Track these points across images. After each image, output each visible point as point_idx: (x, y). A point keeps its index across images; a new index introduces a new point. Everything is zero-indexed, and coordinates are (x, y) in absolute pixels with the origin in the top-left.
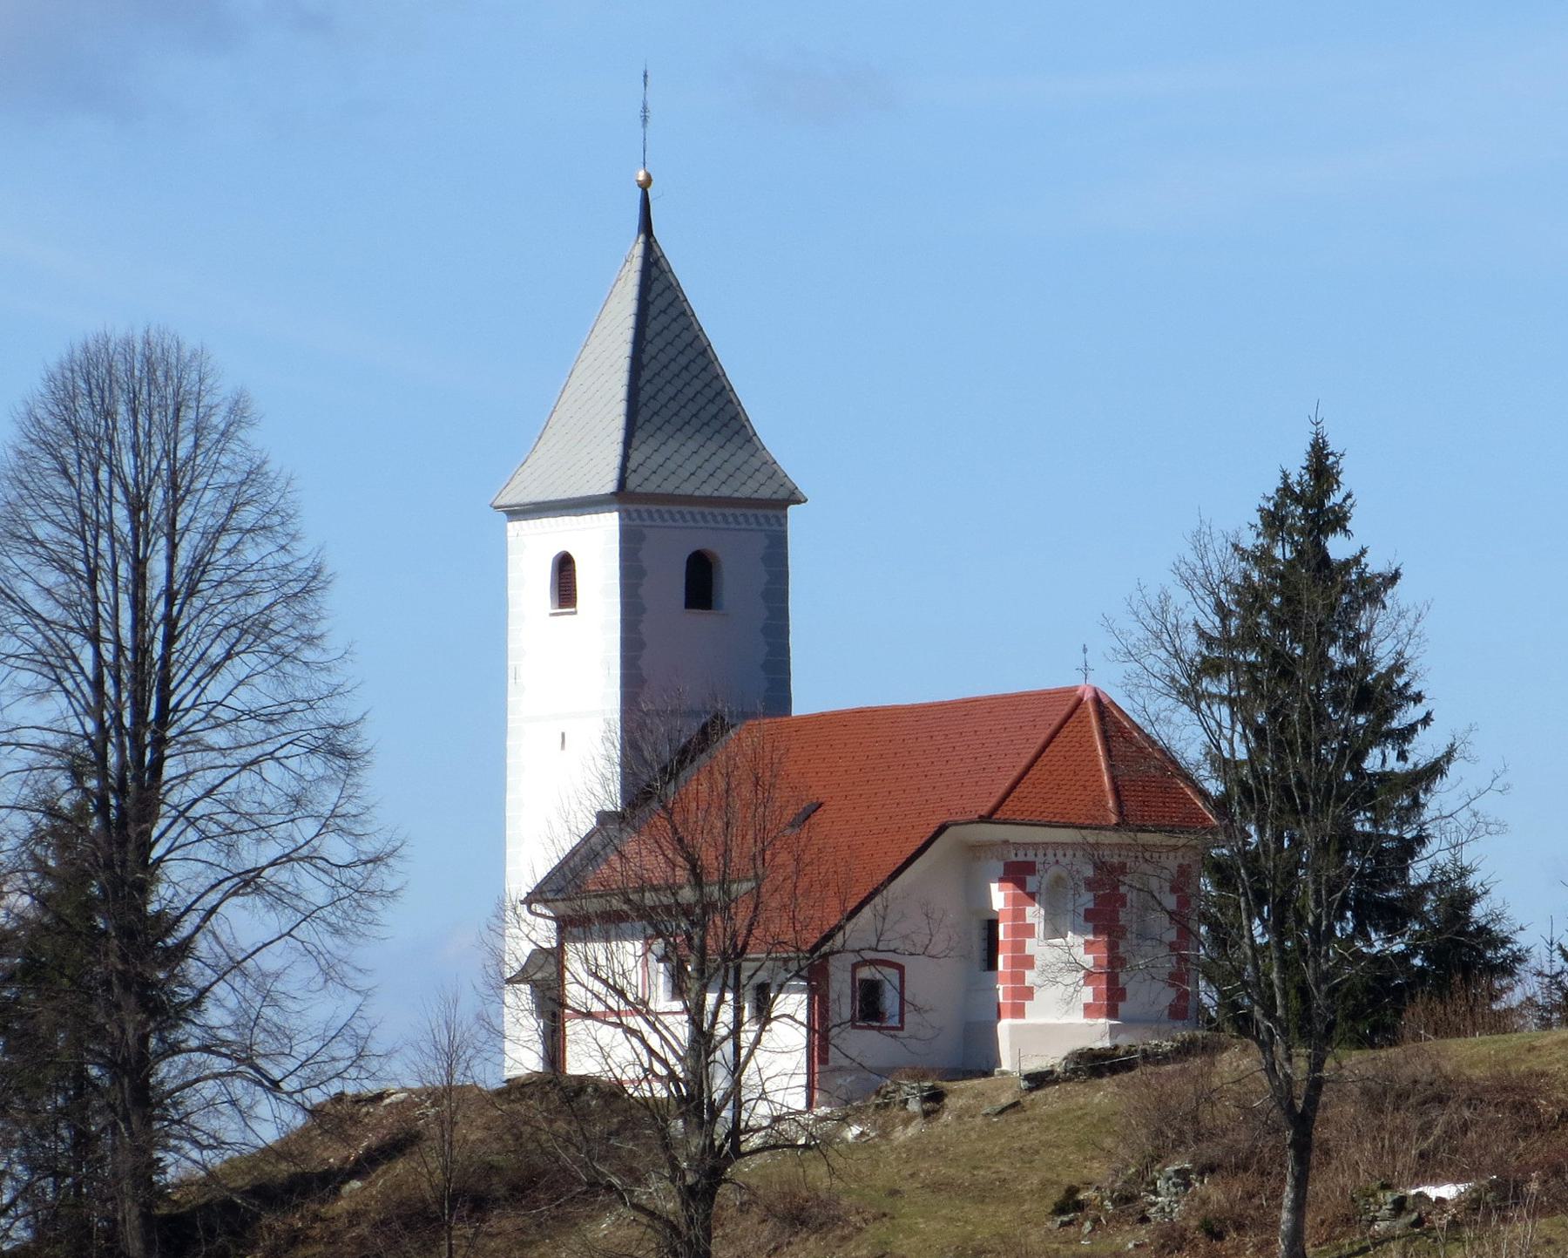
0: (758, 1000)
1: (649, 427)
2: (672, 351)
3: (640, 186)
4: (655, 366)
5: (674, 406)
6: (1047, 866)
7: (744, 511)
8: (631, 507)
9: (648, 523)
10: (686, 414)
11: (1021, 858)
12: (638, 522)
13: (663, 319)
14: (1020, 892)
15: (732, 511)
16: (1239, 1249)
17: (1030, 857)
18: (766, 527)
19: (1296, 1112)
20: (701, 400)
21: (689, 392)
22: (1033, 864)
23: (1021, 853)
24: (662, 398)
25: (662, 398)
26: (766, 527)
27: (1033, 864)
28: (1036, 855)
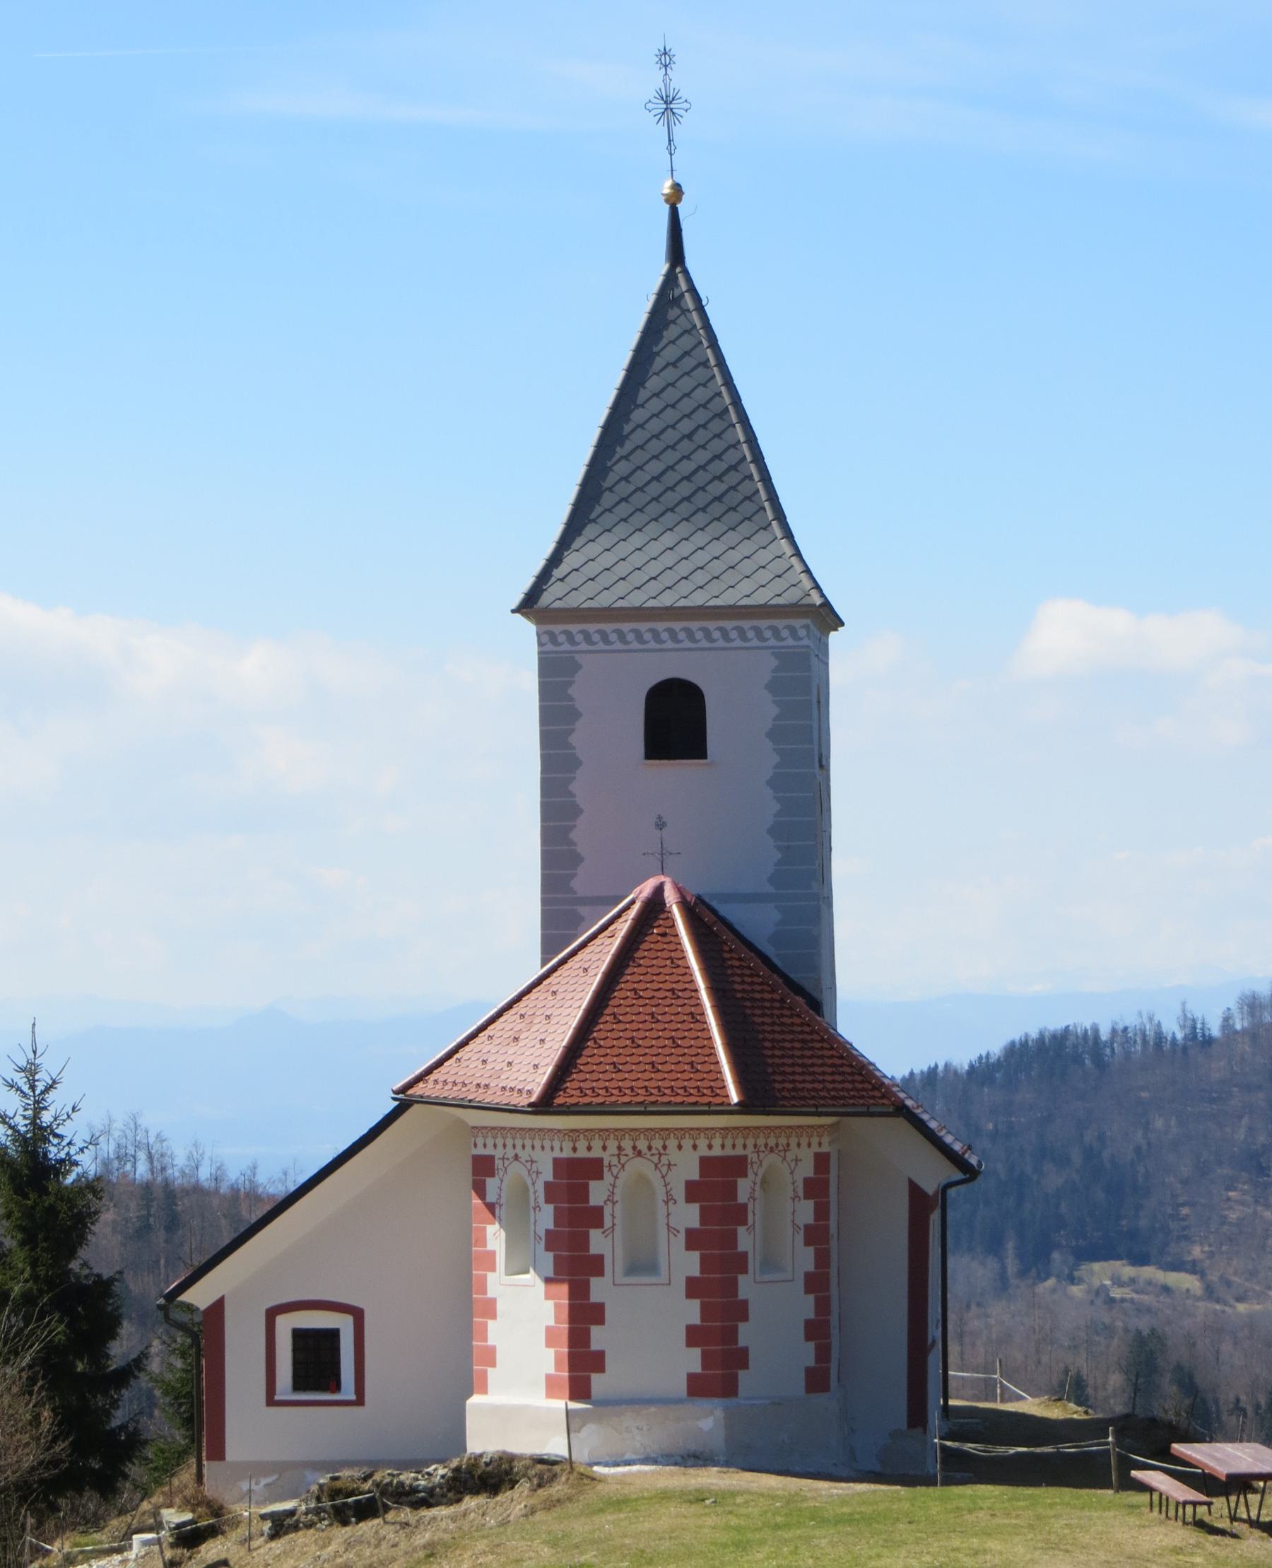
0: (1136, 1390)
1: (608, 519)
2: (670, 415)
3: (667, 201)
4: (639, 437)
5: (655, 489)
6: (623, 1159)
7: (755, 623)
8: (557, 628)
9: (584, 646)
10: (671, 498)
11: (582, 1153)
12: (566, 647)
13: (670, 374)
14: (480, 1201)
15: (734, 623)
16: (393, 1566)
17: (596, 1153)
18: (773, 642)
19: (1222, 1481)
20: (702, 478)
21: (686, 467)
22: (600, 1161)
23: (582, 1145)
24: (640, 478)
25: (640, 478)
26: (773, 642)
27: (599, 1161)
28: (604, 1148)
